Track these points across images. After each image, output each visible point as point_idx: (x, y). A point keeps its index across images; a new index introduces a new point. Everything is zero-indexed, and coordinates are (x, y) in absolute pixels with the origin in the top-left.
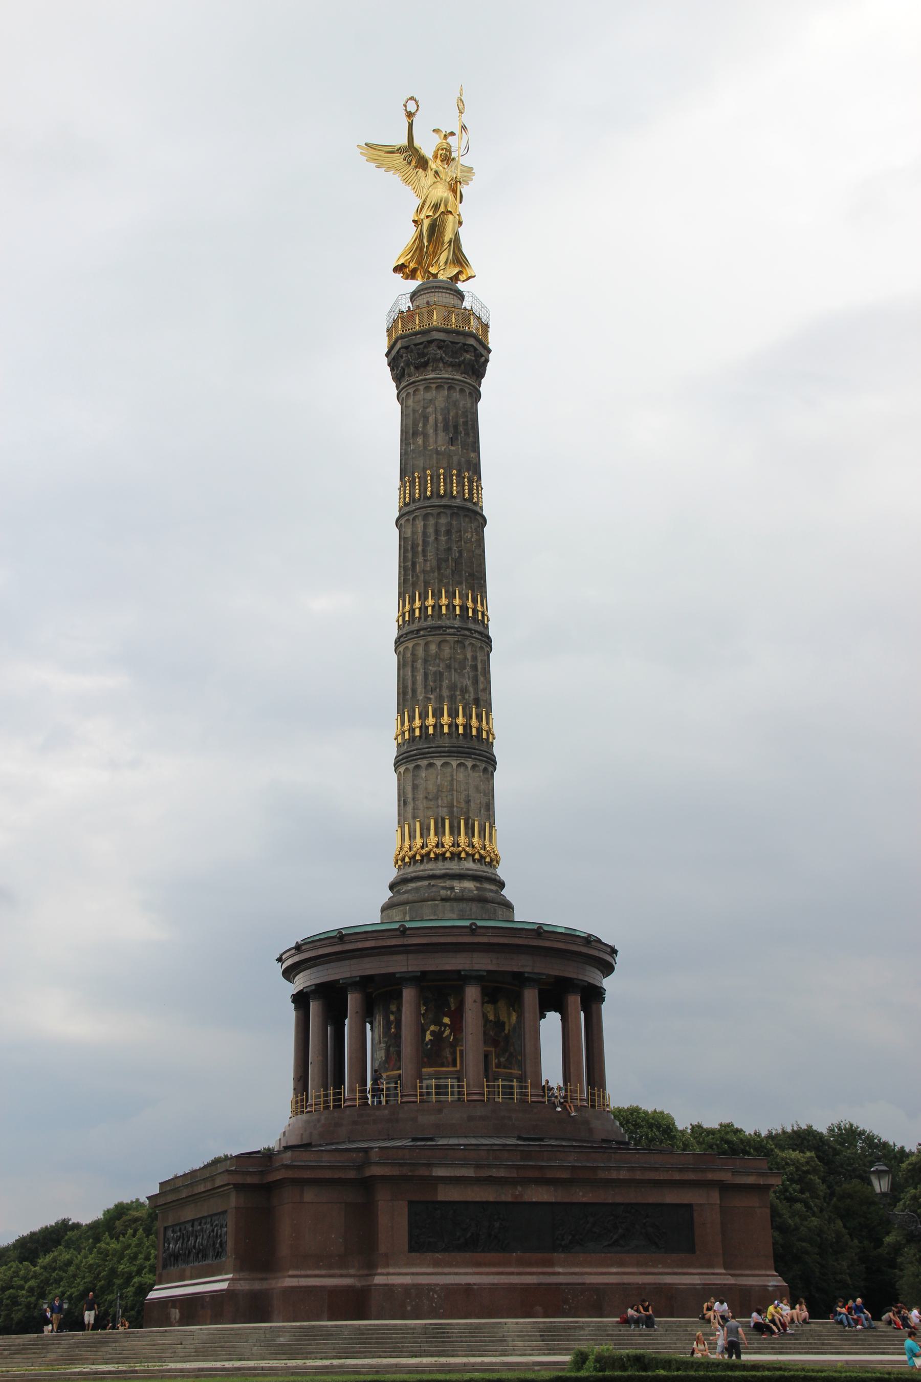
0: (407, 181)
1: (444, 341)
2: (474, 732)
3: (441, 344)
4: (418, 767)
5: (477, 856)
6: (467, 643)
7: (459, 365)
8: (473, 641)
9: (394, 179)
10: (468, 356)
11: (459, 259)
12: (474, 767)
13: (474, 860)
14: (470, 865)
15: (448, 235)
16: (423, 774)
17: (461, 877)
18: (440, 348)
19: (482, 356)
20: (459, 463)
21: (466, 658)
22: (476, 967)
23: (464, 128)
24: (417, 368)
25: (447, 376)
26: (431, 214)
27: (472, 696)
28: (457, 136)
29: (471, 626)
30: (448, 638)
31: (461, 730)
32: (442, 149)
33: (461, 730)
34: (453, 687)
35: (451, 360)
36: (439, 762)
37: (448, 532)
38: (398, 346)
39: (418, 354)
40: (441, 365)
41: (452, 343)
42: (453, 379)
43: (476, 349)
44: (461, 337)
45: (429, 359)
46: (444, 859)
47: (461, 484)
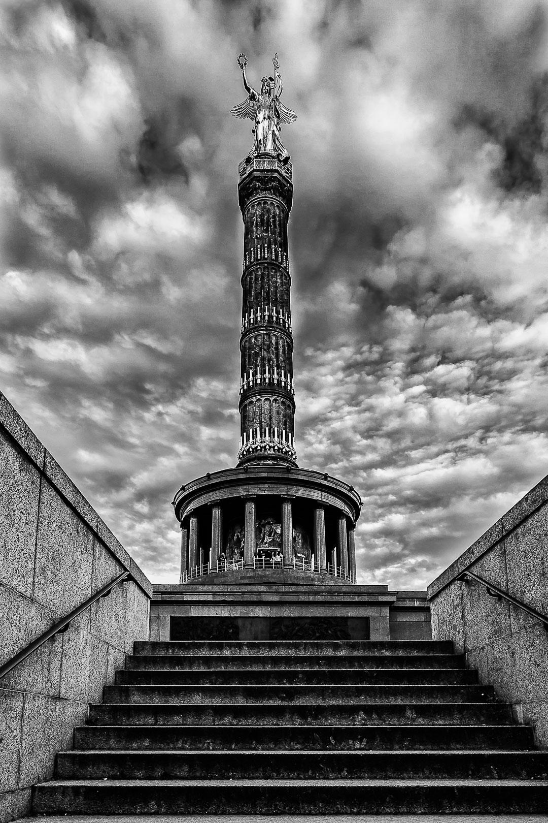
2: (276, 382)
12: (275, 400)
14: (272, 452)
20: (270, 241)
34: (263, 359)
36: (254, 400)
37: (262, 279)
43: (279, 180)
46: (257, 451)
47: (270, 252)
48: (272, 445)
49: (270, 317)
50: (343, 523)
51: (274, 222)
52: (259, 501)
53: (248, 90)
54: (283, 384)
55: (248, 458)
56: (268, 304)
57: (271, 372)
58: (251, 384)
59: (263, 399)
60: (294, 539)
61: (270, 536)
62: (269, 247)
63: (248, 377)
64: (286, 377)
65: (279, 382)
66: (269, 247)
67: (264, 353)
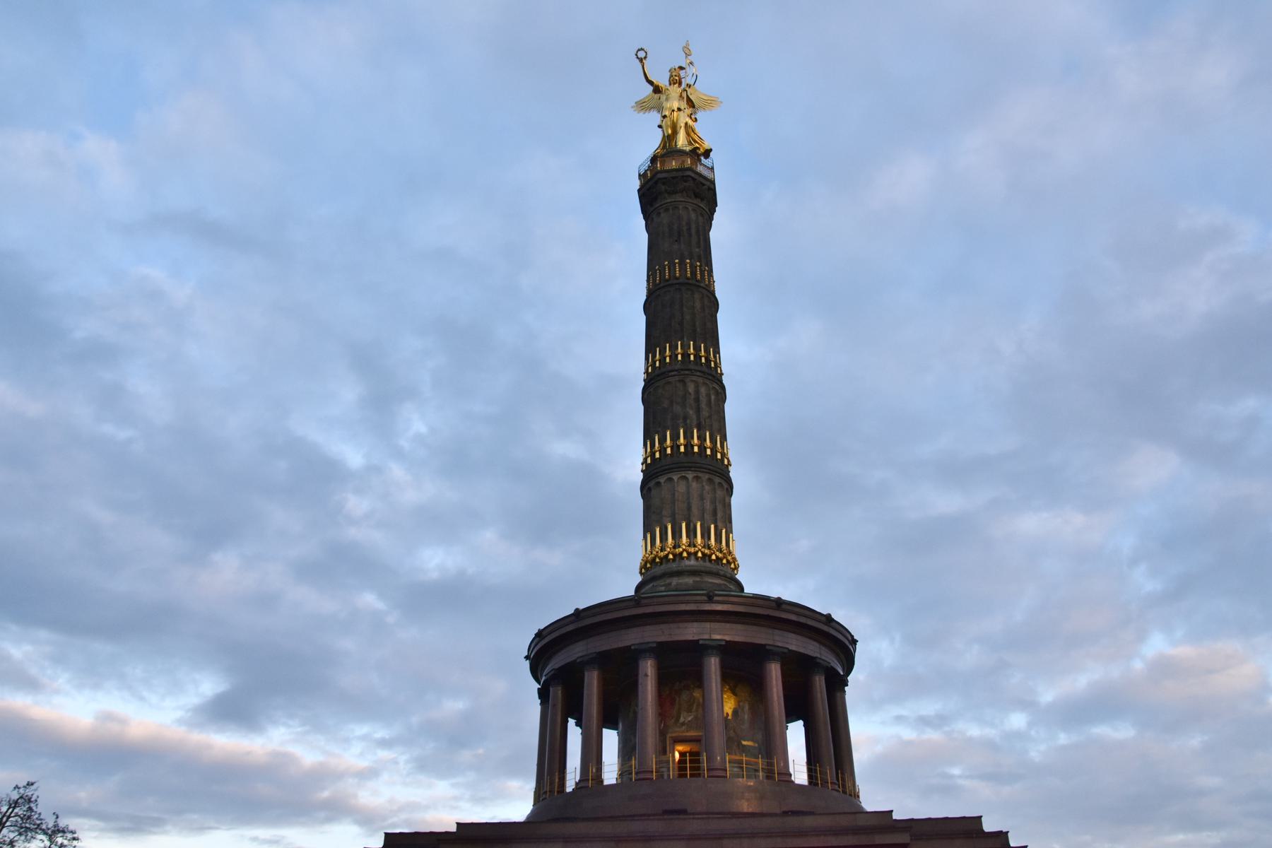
2: (696, 449)
3: (665, 181)
4: (650, 489)
5: (700, 554)
6: (687, 380)
8: (694, 378)
13: (697, 558)
14: (693, 562)
16: (653, 492)
17: (679, 573)
21: (686, 392)
22: (647, 640)
27: (695, 422)
29: (692, 367)
30: (670, 379)
31: (682, 449)
33: (682, 449)
36: (662, 480)
43: (694, 179)
48: (692, 550)
49: (686, 355)
50: (819, 682)
51: (689, 229)
52: (663, 651)
53: (651, 83)
54: (709, 452)
55: (653, 570)
56: (681, 339)
57: (688, 436)
58: (657, 455)
59: (675, 478)
60: (735, 712)
61: (689, 711)
62: (682, 263)
63: (653, 446)
64: (713, 441)
65: (702, 448)
66: (682, 263)
67: (678, 409)
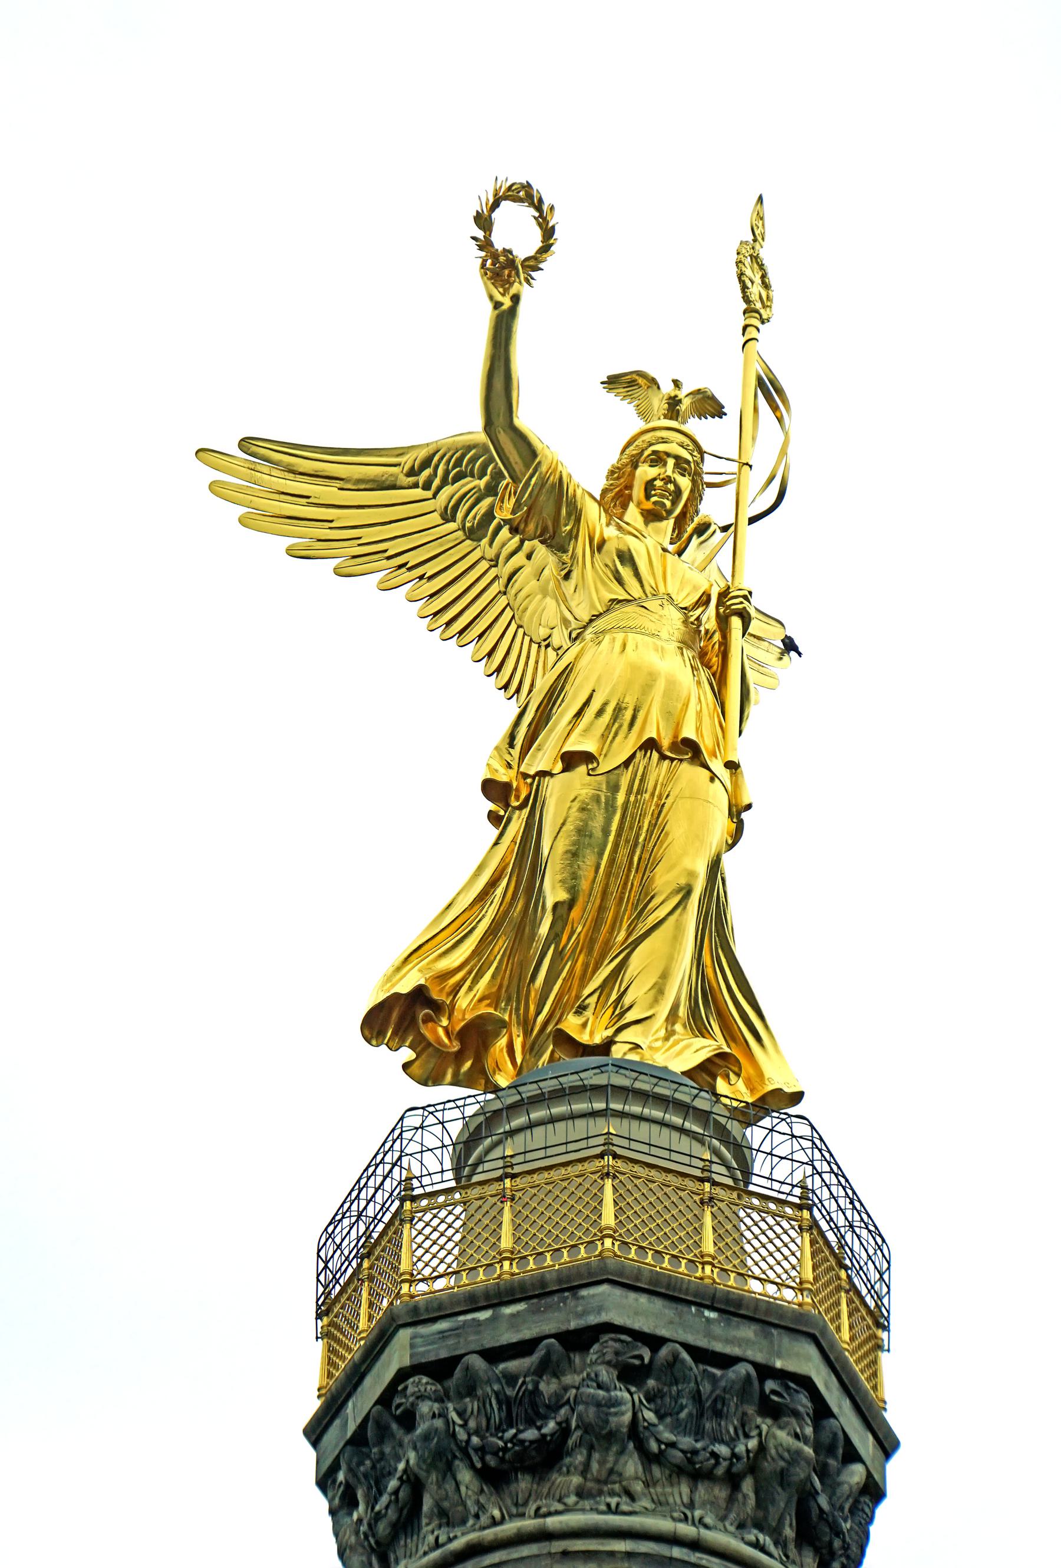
0: (450, 620)
1: (655, 1342)
3: (642, 1361)
7: (733, 1481)
9: (385, 616)
10: (783, 1436)
11: (722, 999)
15: (683, 859)
18: (631, 1374)
19: (852, 1456)
23: (769, 389)
24: (494, 1478)
25: (664, 1525)
26: (590, 746)
28: (728, 424)
32: (658, 459)
35: (686, 1442)
38: (398, 1356)
39: (504, 1401)
40: (632, 1466)
41: (700, 1354)
42: (695, 1545)
44: (748, 1332)
45: (564, 1430)
